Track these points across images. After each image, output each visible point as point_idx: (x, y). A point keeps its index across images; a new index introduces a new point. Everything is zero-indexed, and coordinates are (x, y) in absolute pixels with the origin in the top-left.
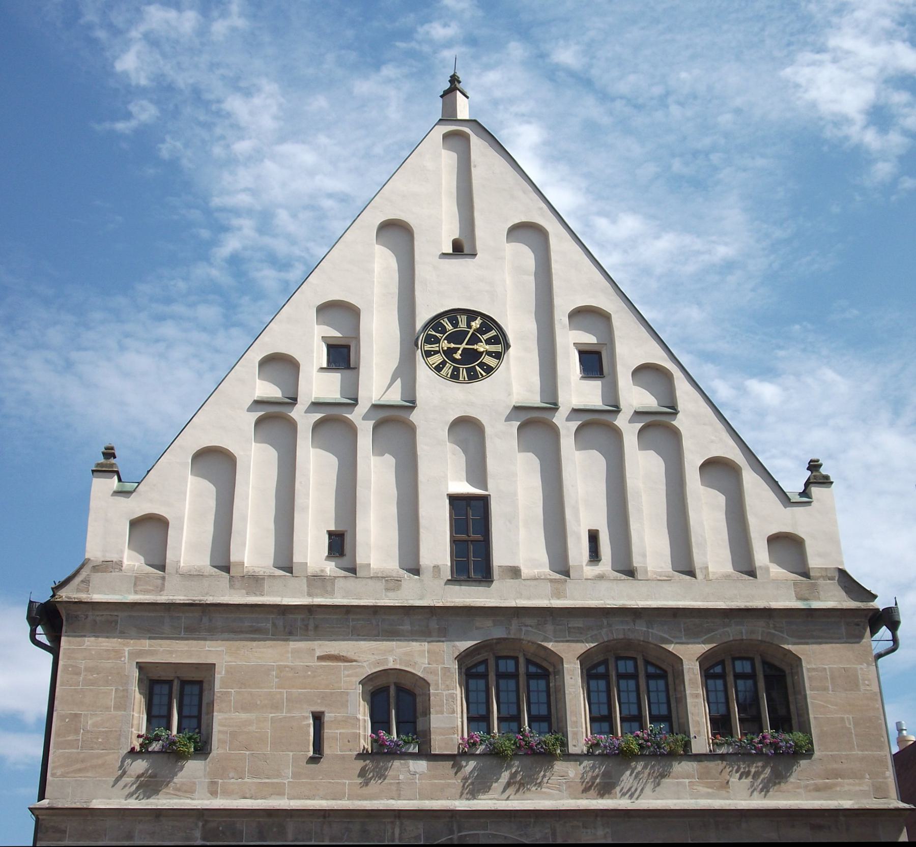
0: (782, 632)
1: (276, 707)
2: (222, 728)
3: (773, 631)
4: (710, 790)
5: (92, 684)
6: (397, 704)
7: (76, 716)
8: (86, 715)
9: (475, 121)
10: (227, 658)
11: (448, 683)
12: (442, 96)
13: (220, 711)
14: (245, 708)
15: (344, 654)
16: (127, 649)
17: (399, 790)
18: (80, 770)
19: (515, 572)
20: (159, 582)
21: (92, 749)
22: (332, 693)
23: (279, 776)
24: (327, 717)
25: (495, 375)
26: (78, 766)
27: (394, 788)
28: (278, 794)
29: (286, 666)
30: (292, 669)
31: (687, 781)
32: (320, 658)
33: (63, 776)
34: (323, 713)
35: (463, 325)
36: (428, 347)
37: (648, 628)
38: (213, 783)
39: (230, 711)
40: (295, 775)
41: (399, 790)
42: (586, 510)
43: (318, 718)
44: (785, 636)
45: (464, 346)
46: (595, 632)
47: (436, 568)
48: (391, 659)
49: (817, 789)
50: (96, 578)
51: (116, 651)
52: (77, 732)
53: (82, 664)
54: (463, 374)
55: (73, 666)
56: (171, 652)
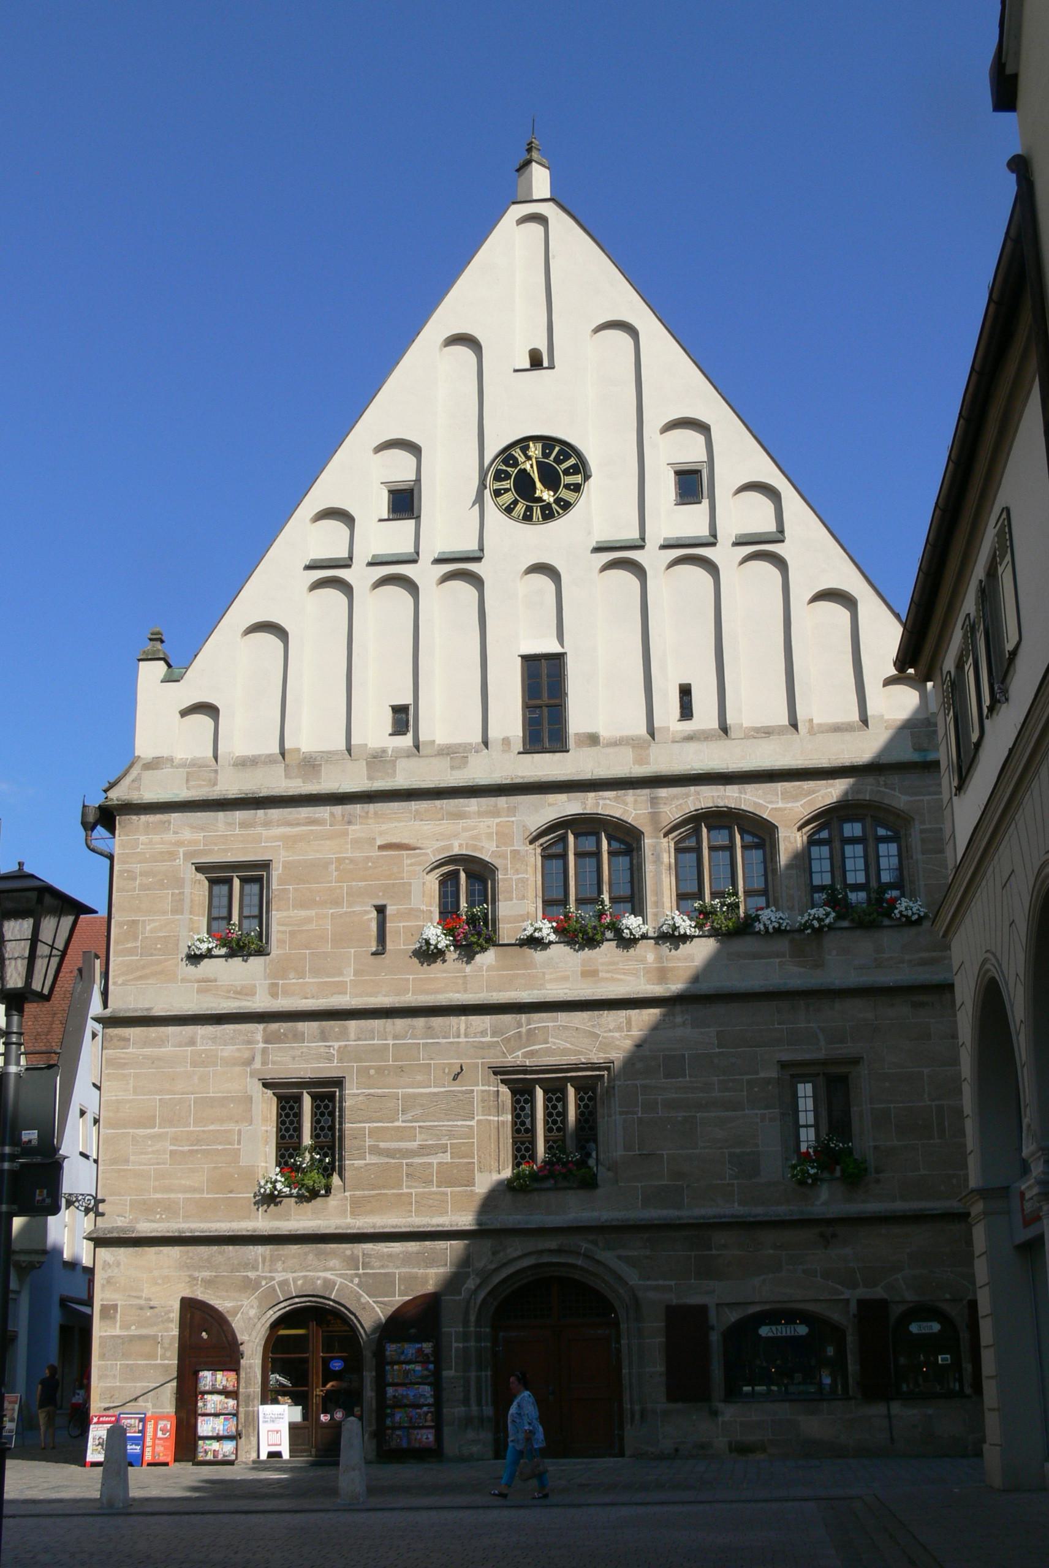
0: (894, 789)
1: (336, 903)
3: (883, 789)
4: (802, 970)
5: (149, 889)
8: (144, 921)
10: (283, 853)
11: (518, 866)
14: (302, 905)
16: (181, 850)
17: (465, 983)
19: (593, 739)
20: (212, 775)
22: (393, 884)
23: (341, 974)
24: (390, 910)
25: (573, 513)
26: (139, 974)
27: (460, 981)
28: (340, 994)
29: (345, 858)
30: (352, 861)
31: (778, 960)
32: (382, 848)
33: (123, 984)
36: (498, 485)
37: (741, 793)
39: (288, 909)
41: (465, 983)
42: (682, 659)
43: (381, 910)
44: (897, 794)
46: (681, 801)
47: (506, 741)
48: (456, 844)
49: (924, 963)
50: (148, 775)
51: (170, 853)
52: (136, 939)
53: (138, 868)
56: (226, 851)
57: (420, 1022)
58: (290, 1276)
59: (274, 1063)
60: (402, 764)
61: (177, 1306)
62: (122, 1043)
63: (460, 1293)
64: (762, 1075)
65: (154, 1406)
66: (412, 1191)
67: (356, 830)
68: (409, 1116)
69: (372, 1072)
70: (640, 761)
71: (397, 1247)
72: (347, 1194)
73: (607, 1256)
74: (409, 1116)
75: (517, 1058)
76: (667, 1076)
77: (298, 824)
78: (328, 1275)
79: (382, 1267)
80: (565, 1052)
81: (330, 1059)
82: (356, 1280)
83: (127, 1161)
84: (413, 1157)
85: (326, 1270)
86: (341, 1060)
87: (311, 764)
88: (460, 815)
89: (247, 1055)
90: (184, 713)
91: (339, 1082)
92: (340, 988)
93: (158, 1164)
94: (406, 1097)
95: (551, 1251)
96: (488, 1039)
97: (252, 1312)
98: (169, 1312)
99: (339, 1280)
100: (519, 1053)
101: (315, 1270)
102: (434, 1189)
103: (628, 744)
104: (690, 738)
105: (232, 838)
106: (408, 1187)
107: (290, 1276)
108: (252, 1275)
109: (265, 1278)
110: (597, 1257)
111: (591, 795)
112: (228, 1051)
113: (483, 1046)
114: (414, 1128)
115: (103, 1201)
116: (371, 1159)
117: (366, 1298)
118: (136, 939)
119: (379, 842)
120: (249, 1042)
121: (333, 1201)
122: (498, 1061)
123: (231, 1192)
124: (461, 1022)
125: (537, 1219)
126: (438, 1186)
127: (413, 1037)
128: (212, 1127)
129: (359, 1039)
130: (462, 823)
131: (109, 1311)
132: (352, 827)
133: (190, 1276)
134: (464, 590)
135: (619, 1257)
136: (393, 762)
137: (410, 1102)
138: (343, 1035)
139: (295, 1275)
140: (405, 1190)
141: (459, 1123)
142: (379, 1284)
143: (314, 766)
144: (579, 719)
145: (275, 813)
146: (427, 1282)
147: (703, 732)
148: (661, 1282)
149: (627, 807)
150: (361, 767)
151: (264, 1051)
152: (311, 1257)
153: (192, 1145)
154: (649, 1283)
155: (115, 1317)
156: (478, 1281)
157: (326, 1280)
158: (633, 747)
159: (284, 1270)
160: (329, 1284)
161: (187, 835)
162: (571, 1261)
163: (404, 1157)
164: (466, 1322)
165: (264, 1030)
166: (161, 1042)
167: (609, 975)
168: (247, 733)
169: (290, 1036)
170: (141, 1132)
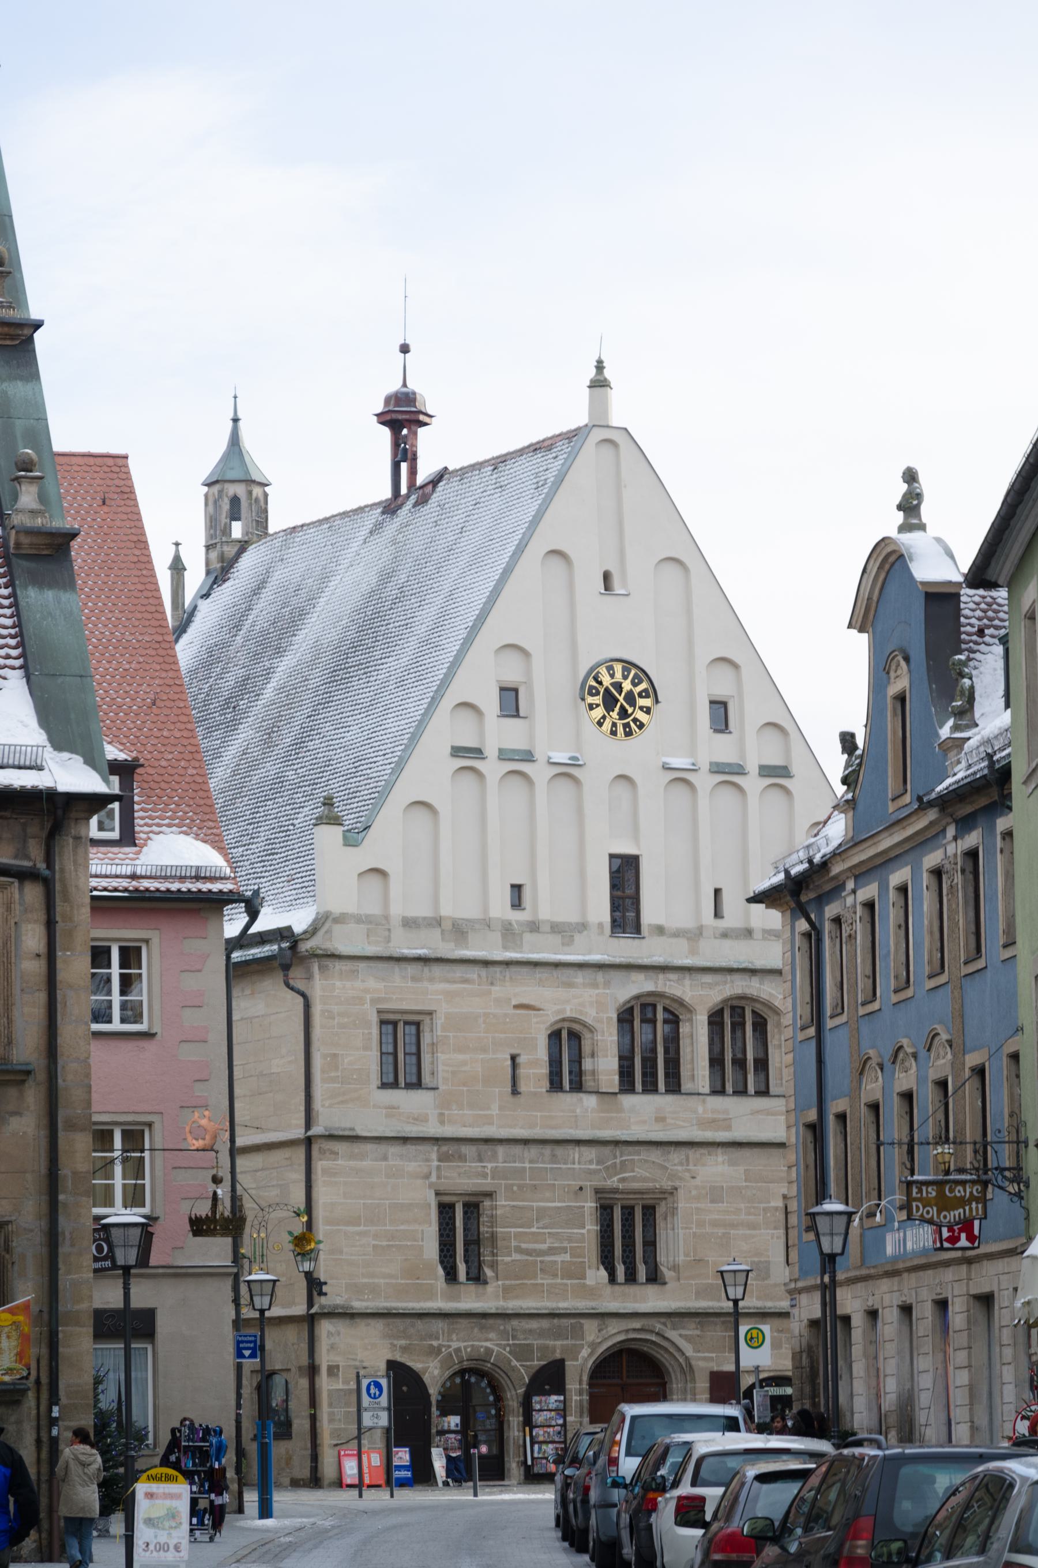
1: (484, 1050)
2: (446, 1068)
6: (567, 1043)
7: (335, 1055)
9: (626, 429)
12: (589, 387)
13: (442, 1053)
15: (532, 1003)
16: (368, 996)
18: (342, 1102)
19: (660, 930)
20: (387, 933)
21: (350, 1084)
23: (489, 1108)
24: (521, 1060)
28: (489, 1124)
32: (516, 1007)
33: (331, 1106)
34: (518, 1055)
35: (618, 676)
38: (442, 1114)
40: (501, 1108)
43: (513, 1058)
45: (621, 698)
46: (721, 987)
47: (601, 925)
48: (568, 1008)
50: (337, 928)
52: (337, 1069)
54: (620, 730)
55: (329, 1011)
57: (547, 1150)
58: (462, 1345)
59: (446, 1178)
60: (528, 937)
61: (383, 1366)
62: (333, 1156)
63: (577, 1360)
64: (773, 1204)
65: (369, 1442)
66: (545, 1282)
67: (497, 990)
68: (541, 1224)
69: (515, 1188)
70: (693, 952)
71: (534, 1324)
72: (500, 1283)
73: (672, 1335)
74: (541, 1224)
75: (613, 1182)
76: (712, 1201)
77: (455, 982)
78: (488, 1344)
79: (525, 1339)
80: (645, 1180)
81: (485, 1176)
82: (508, 1349)
83: (341, 1252)
84: (543, 1256)
85: (487, 1340)
86: (493, 1178)
87: (459, 930)
88: (570, 985)
89: (426, 1170)
90: (360, 875)
91: (489, 1195)
92: (489, 1121)
93: (364, 1255)
94: (539, 1209)
95: (634, 1330)
96: (593, 1167)
97: (436, 1372)
98: (377, 1371)
99: (496, 1349)
100: (615, 1179)
101: (479, 1340)
102: (559, 1281)
103: (684, 936)
104: (725, 935)
105: (405, 992)
106: (542, 1279)
107: (462, 1345)
108: (435, 1343)
109: (444, 1346)
110: (666, 1335)
111: (661, 976)
112: (412, 1166)
113: (591, 1172)
114: (544, 1233)
115: (325, 1283)
116: (516, 1256)
117: (514, 1363)
118: (337, 1069)
119: (514, 1002)
120: (427, 1160)
121: (490, 1289)
122: (600, 1184)
123: (418, 1279)
124: (575, 1153)
125: (630, 1307)
126: (562, 1279)
127: (543, 1162)
128: (402, 1227)
129: (505, 1162)
130: (573, 991)
131: (333, 1371)
132: (493, 988)
133: (391, 1344)
134: (565, 787)
135: (680, 1335)
136: (521, 935)
137: (542, 1213)
138: (494, 1158)
139: (466, 1344)
140: (540, 1281)
141: (575, 1231)
142: (523, 1352)
143: (463, 933)
144: (651, 912)
145: (437, 970)
146: (555, 1351)
147: (733, 930)
148: (706, 1355)
149: (683, 989)
150: (496, 937)
151: (438, 1168)
152: (476, 1330)
153: (389, 1240)
154: (699, 1355)
155: (338, 1375)
156: (589, 1350)
157: (487, 1348)
158: (688, 939)
159: (458, 1340)
160: (489, 1351)
161: (372, 983)
162: (648, 1337)
163: (538, 1255)
164: (581, 1382)
165: (438, 1151)
166: (362, 1157)
167: (673, 1121)
168: (406, 899)
169: (456, 1156)
170: (351, 1229)
